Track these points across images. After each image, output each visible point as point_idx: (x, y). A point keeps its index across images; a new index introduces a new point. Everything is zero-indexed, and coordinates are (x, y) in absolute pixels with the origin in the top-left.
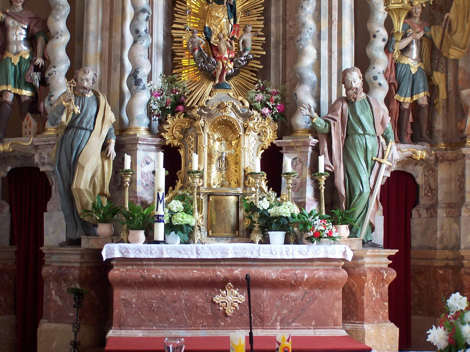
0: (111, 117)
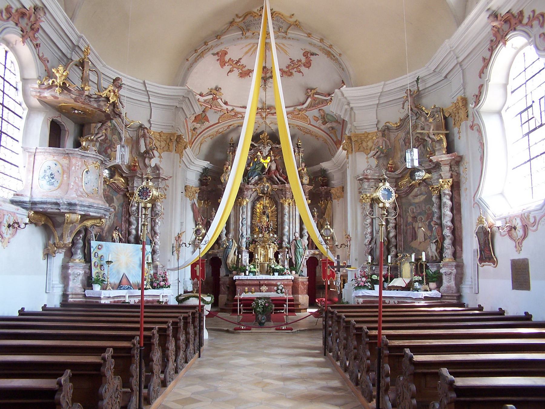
0: (236, 245)
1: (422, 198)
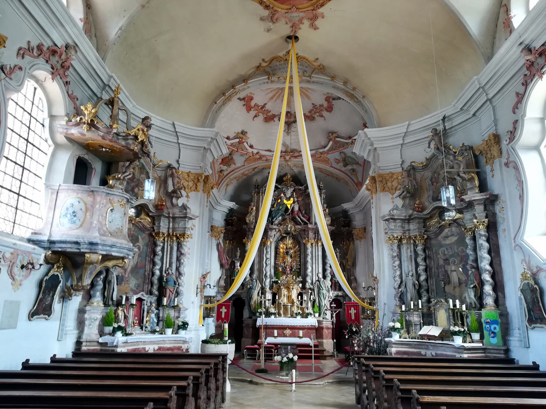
0: (260, 285)
1: (454, 239)
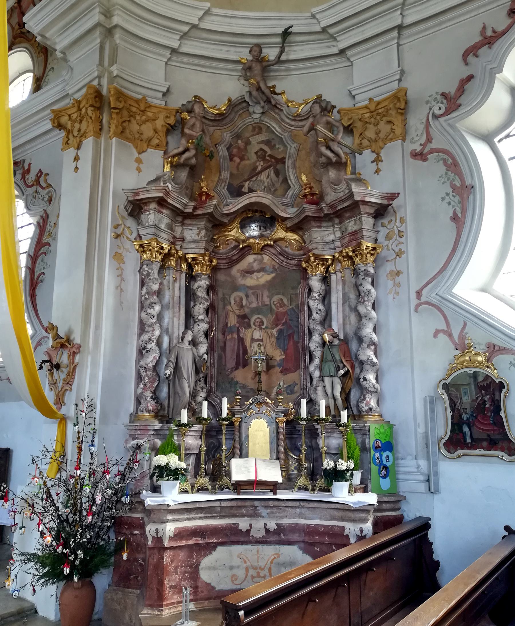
1: (265, 278)
